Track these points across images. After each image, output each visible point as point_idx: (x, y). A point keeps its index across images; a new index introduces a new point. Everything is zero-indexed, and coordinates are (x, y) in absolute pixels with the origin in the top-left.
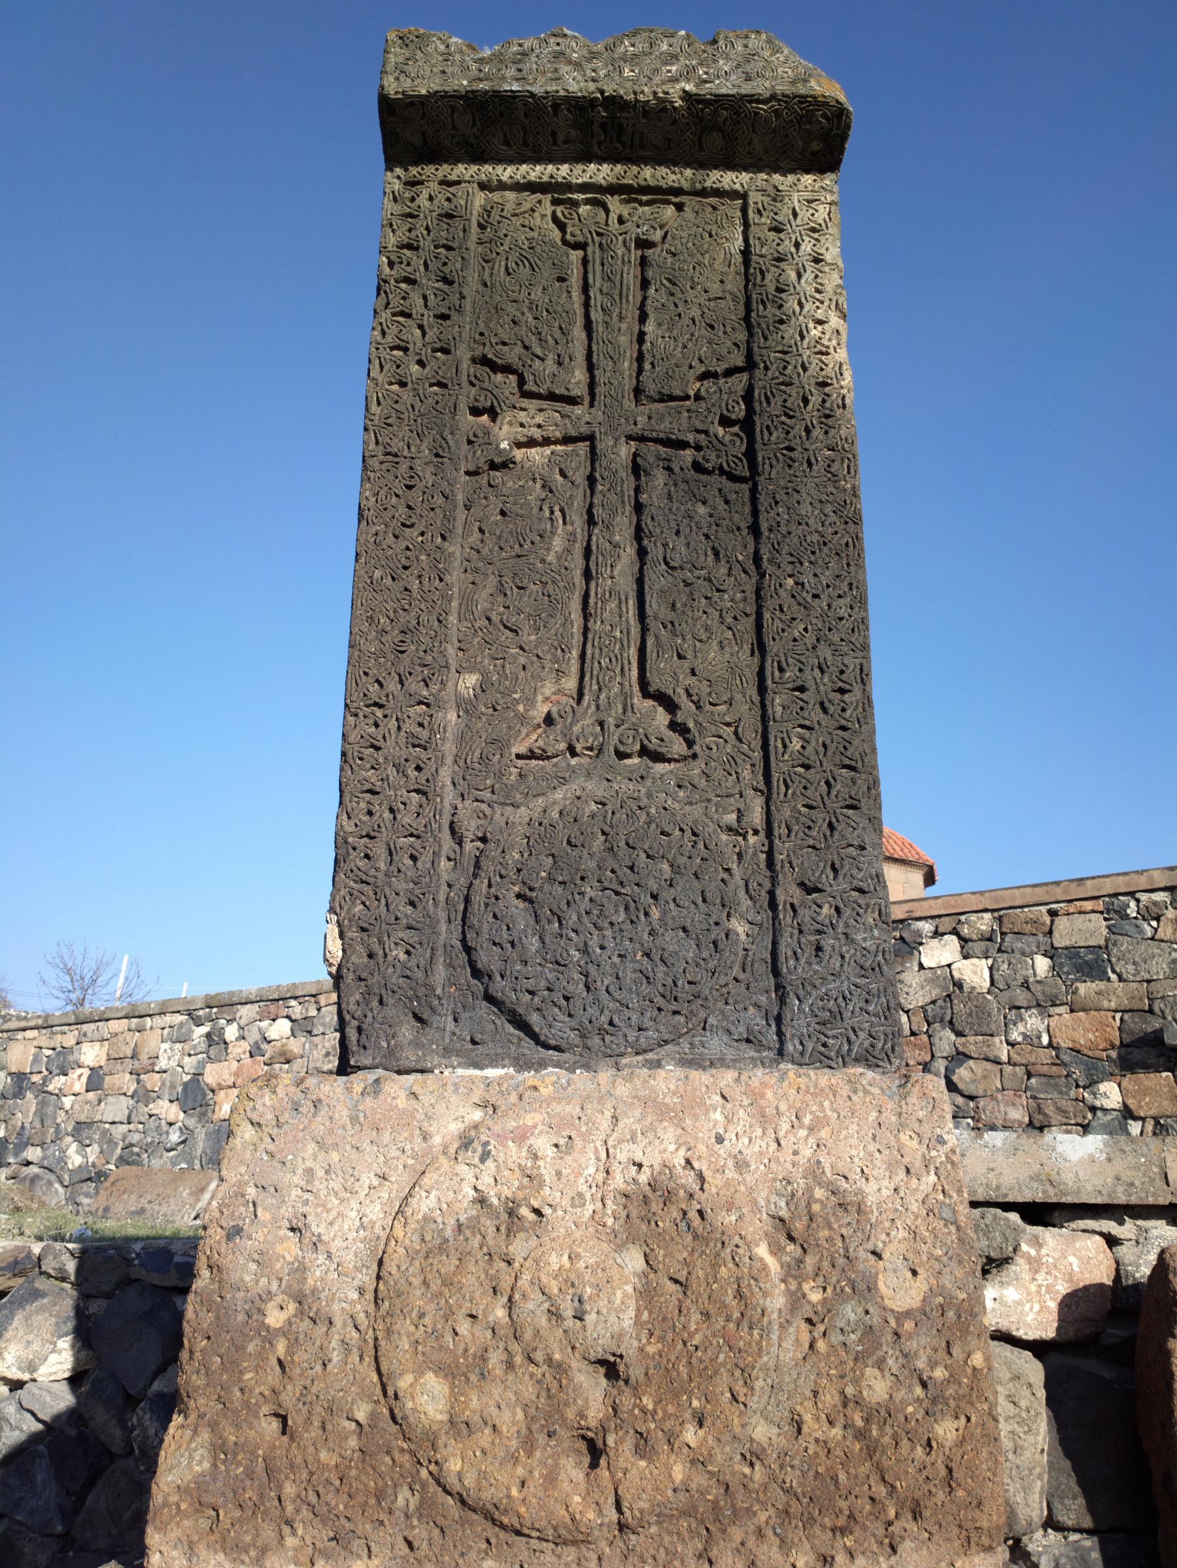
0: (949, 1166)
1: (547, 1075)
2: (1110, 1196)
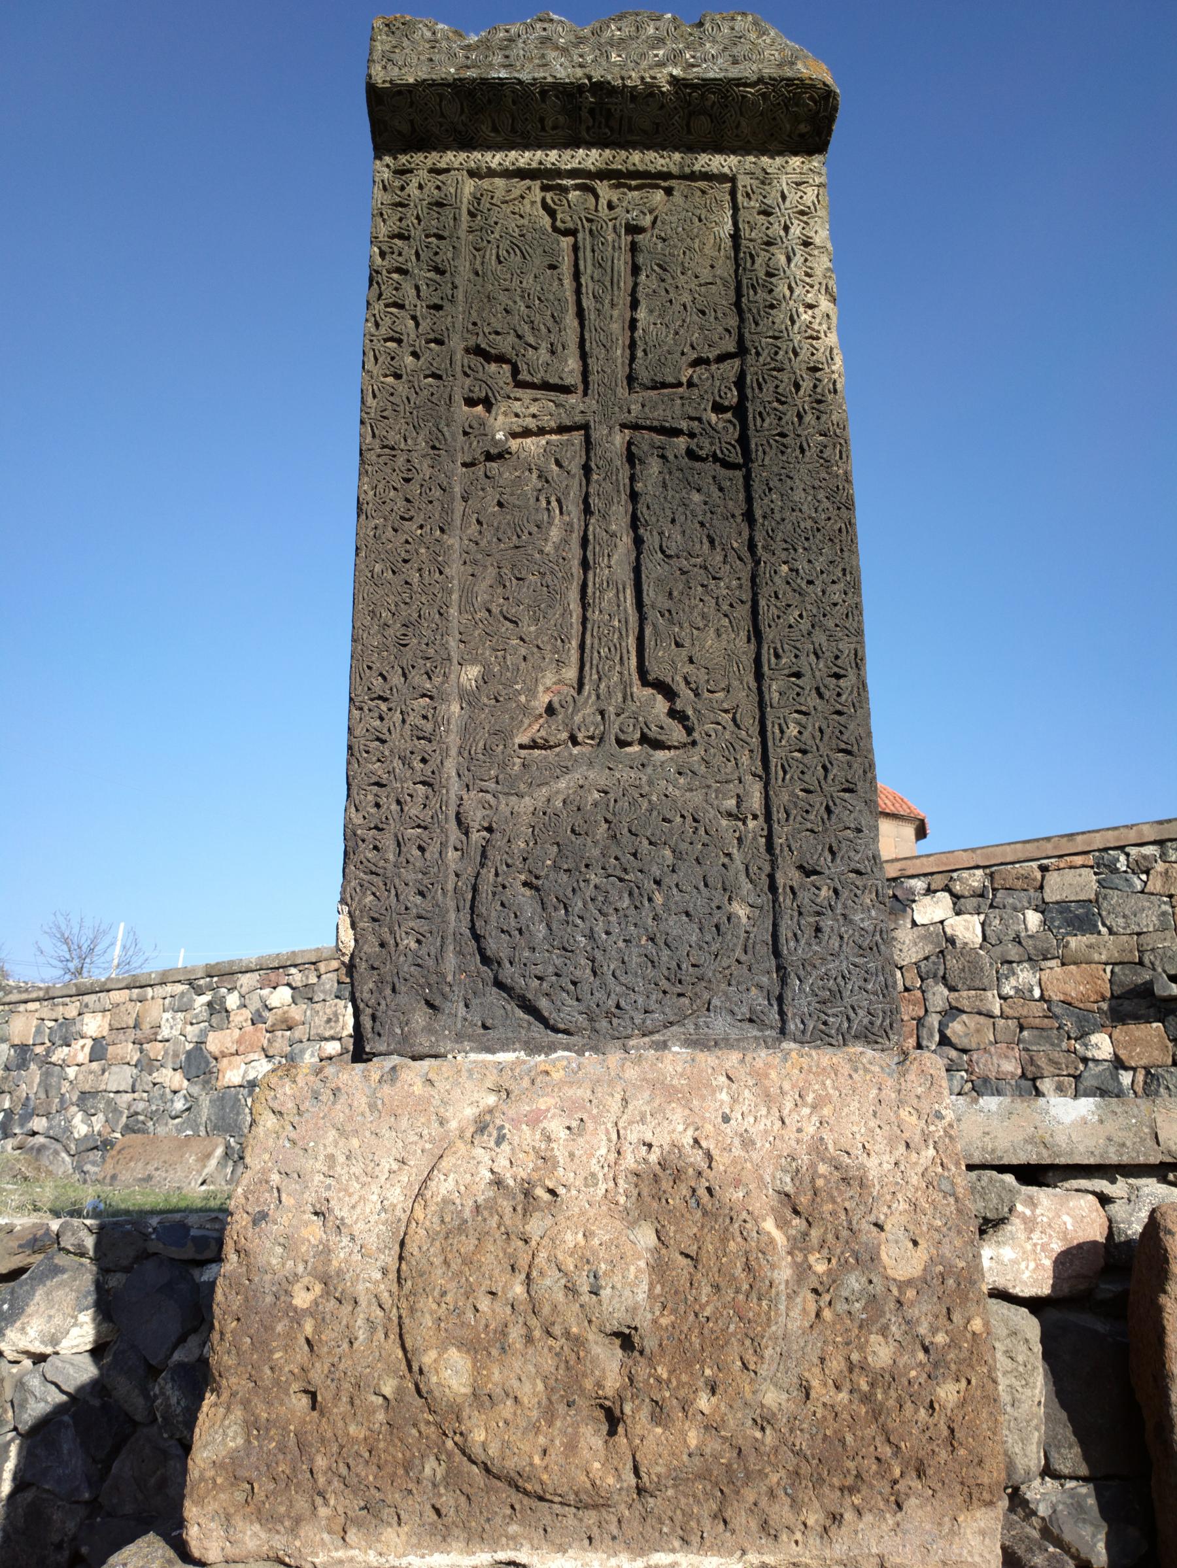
0: (947, 1140)
1: (558, 1059)
2: (1102, 1156)
